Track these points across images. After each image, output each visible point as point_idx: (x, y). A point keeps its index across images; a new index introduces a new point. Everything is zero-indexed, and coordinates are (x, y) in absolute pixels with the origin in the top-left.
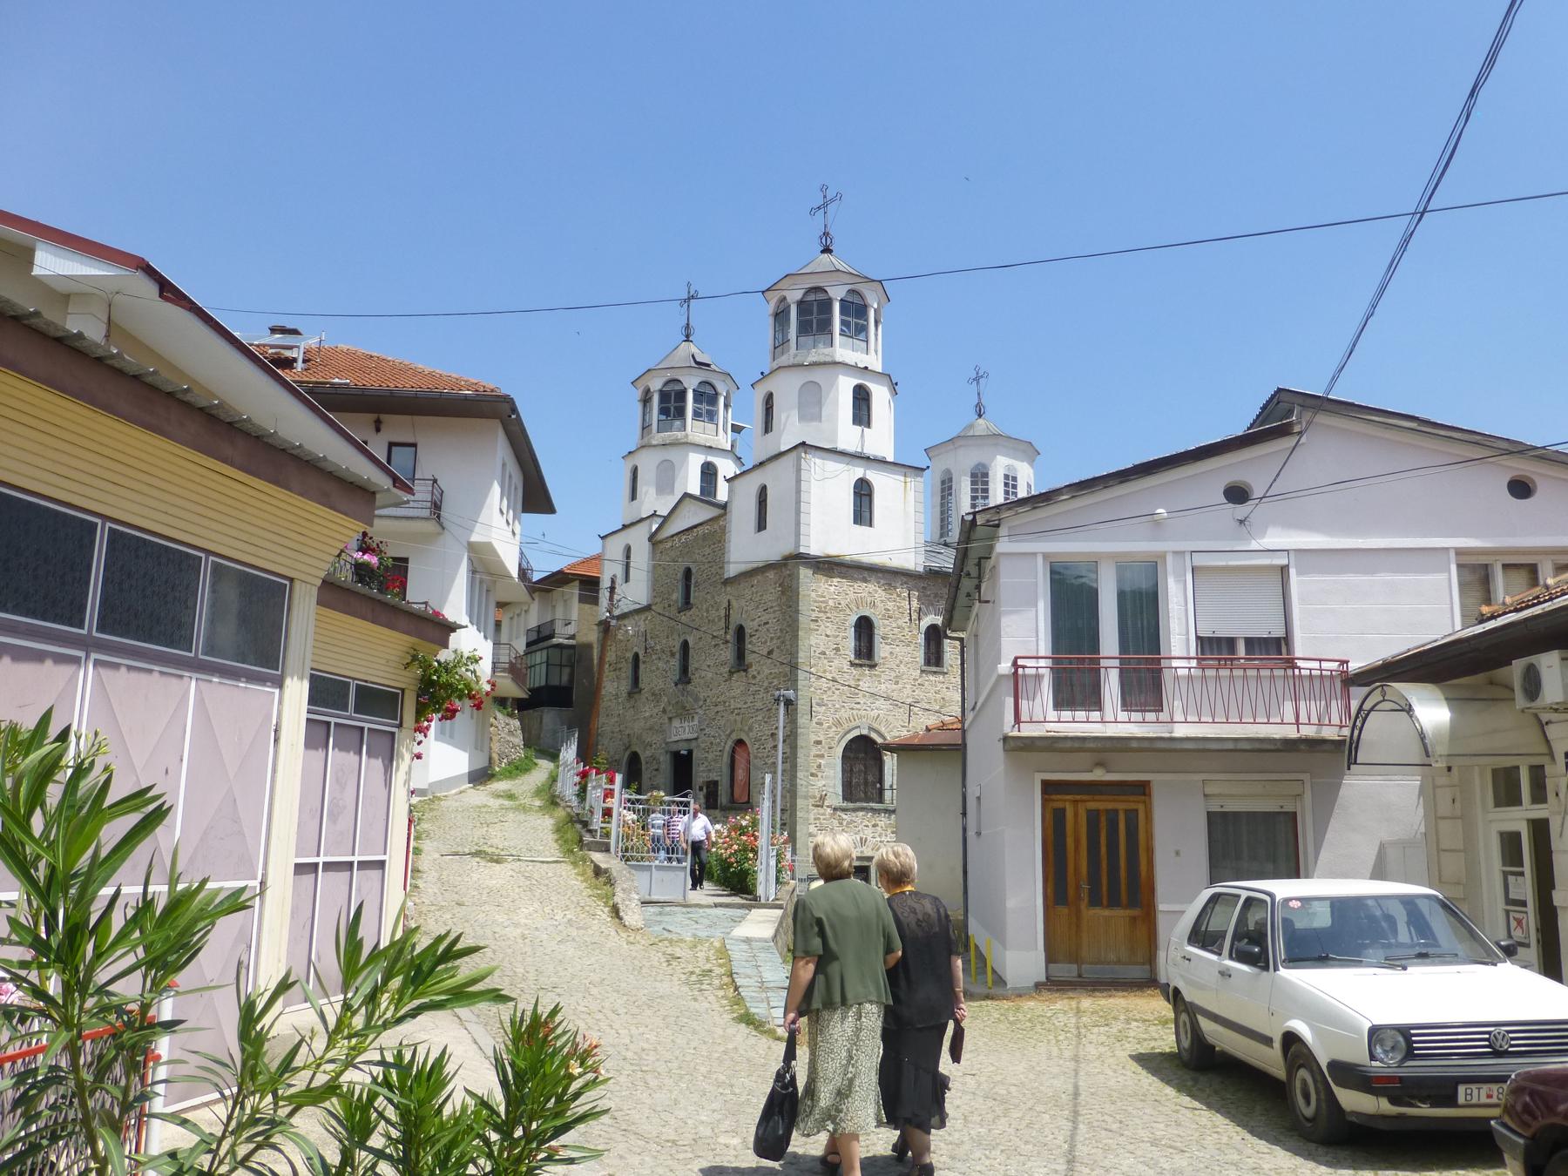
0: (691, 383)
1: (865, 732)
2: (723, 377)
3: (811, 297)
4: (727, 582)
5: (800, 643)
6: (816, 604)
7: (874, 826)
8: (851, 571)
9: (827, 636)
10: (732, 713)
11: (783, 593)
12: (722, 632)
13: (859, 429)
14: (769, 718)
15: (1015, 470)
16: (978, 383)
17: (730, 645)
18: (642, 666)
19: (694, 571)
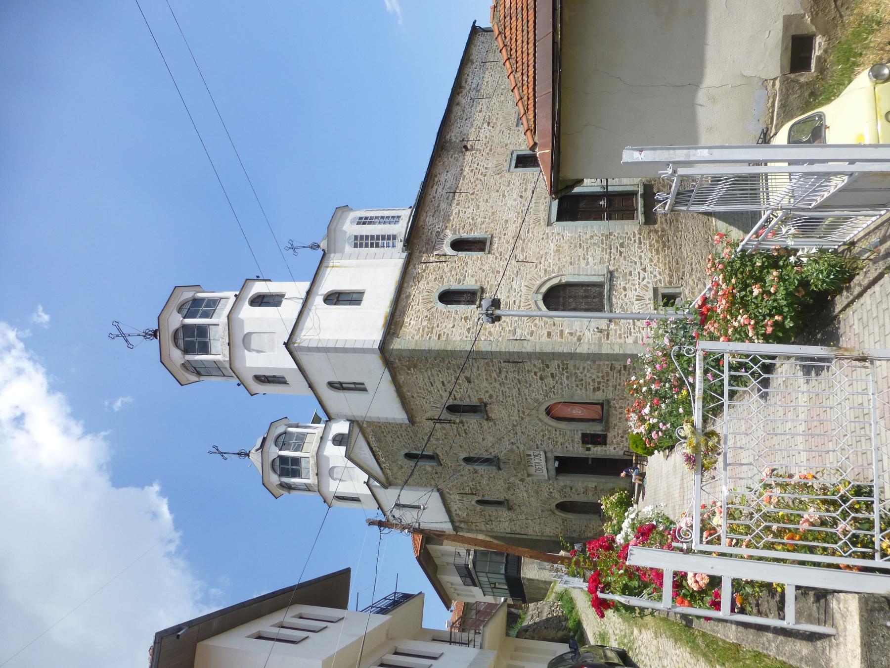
0: (274, 452)
1: (540, 297)
2: (273, 429)
3: (181, 343)
4: (412, 420)
5: (458, 349)
6: (425, 335)
7: (625, 289)
8: (400, 307)
9: (453, 327)
10: (522, 419)
11: (415, 366)
12: (454, 426)
13: (284, 302)
14: (526, 382)
15: (354, 218)
16: (296, 248)
17: (464, 420)
18: (486, 498)
19: (407, 451)
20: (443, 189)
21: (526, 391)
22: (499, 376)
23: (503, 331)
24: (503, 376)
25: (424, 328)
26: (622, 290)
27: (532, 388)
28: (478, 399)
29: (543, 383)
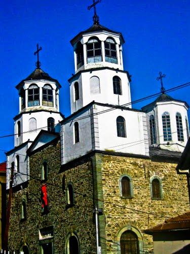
1: (129, 229)
3: (92, 41)
13: (117, 95)
25: (108, 171)
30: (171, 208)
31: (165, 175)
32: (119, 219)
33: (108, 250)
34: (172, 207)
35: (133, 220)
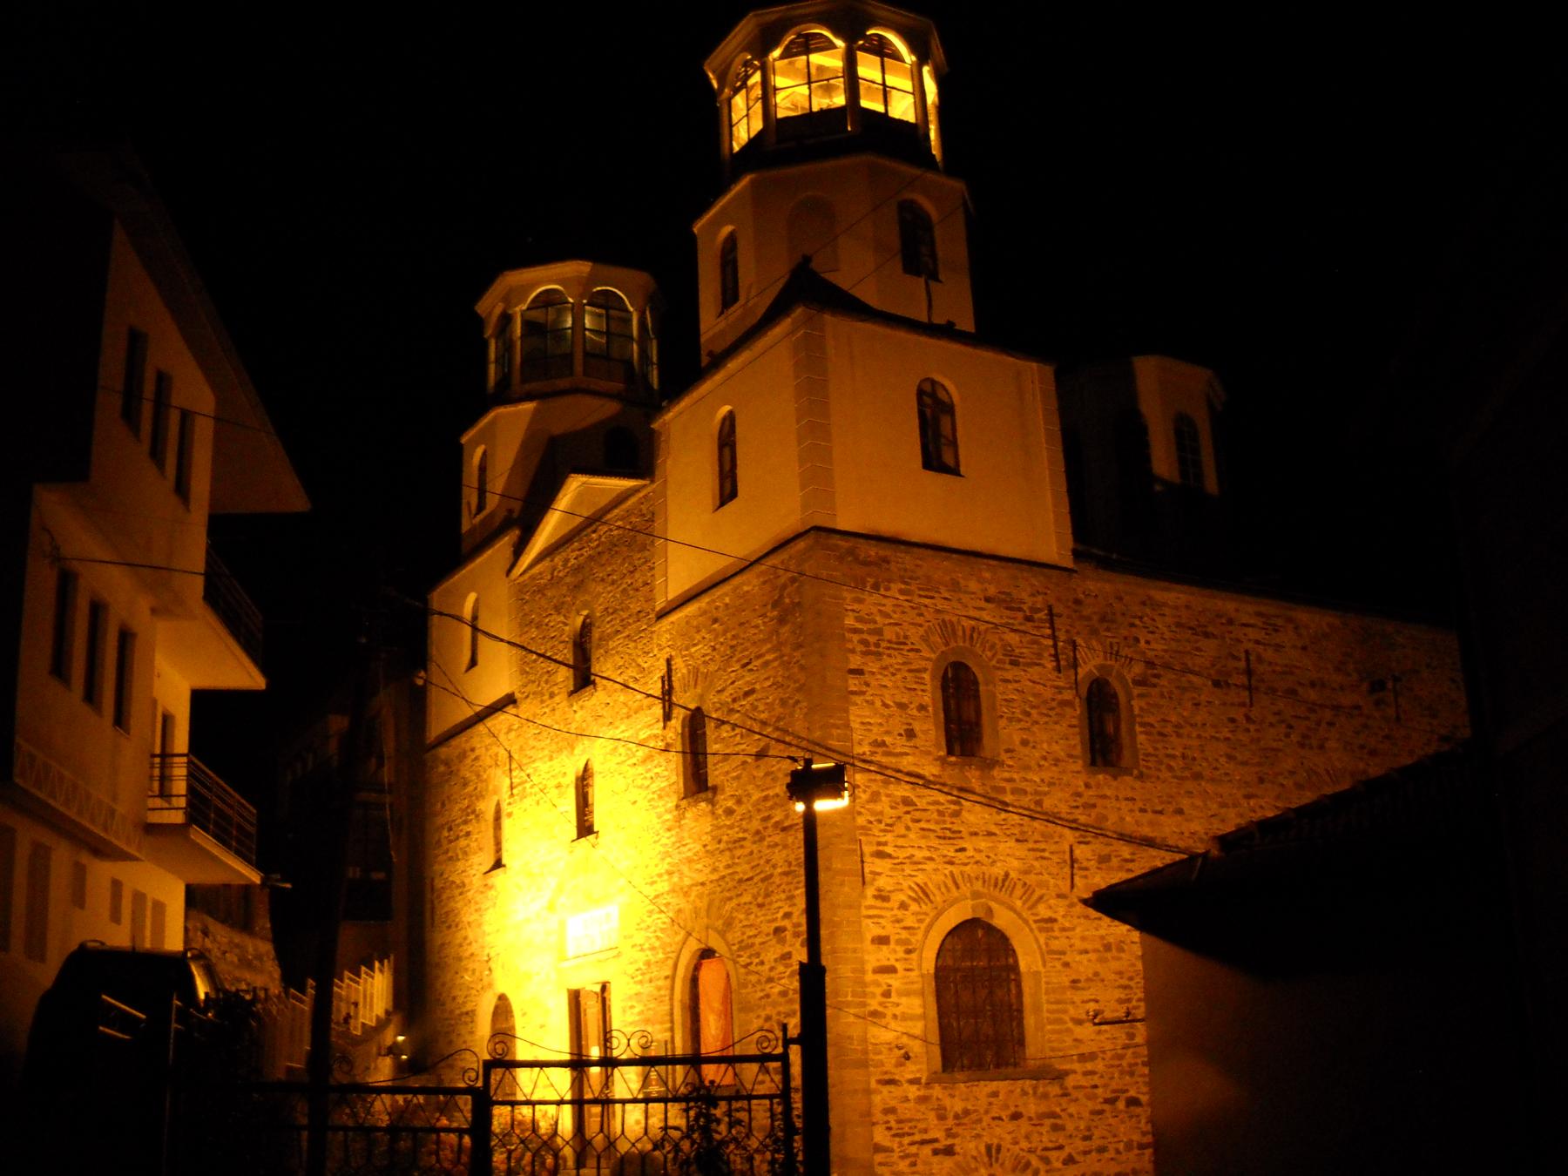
6: (856, 638)
7: (1016, 1116)
11: (782, 621)
14: (767, 895)
20: (1257, 642)
21: (746, 898)
22: (777, 824)
23: (882, 826)
24: (777, 839)
25: (879, 632)
26: (1013, 1109)
27: (755, 909)
28: (722, 781)
29: (768, 935)
30: (1179, 818)
31: (1150, 664)
32: (929, 866)
33: (875, 1014)
34: (1180, 812)
35: (999, 871)
